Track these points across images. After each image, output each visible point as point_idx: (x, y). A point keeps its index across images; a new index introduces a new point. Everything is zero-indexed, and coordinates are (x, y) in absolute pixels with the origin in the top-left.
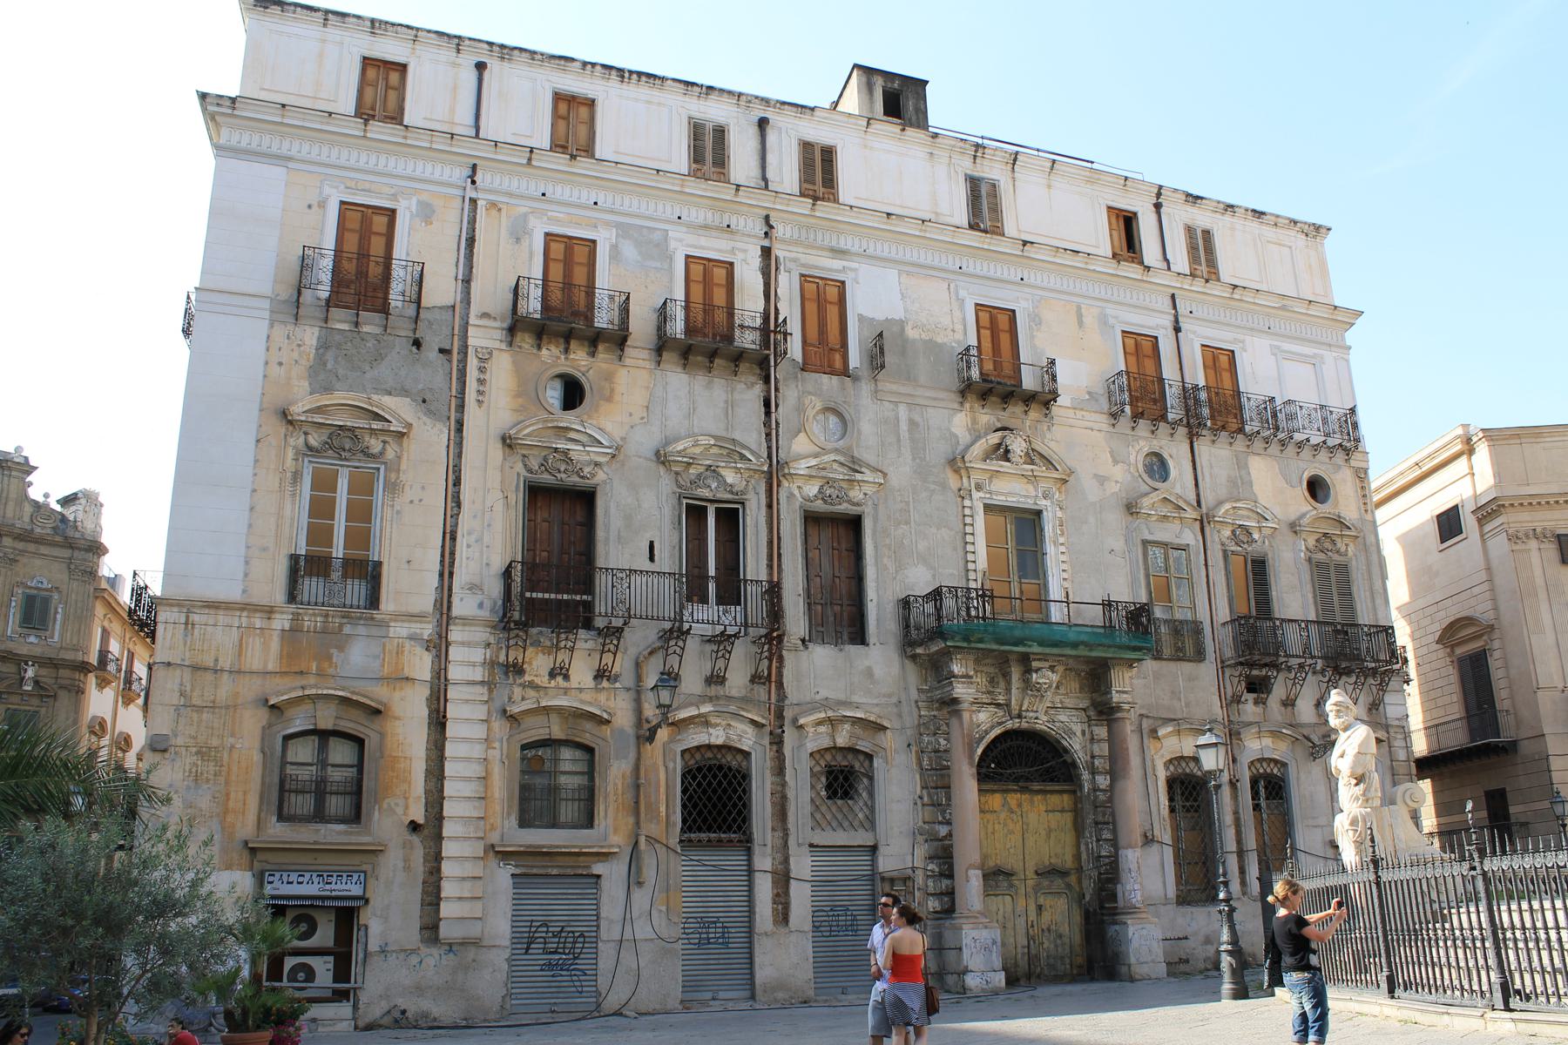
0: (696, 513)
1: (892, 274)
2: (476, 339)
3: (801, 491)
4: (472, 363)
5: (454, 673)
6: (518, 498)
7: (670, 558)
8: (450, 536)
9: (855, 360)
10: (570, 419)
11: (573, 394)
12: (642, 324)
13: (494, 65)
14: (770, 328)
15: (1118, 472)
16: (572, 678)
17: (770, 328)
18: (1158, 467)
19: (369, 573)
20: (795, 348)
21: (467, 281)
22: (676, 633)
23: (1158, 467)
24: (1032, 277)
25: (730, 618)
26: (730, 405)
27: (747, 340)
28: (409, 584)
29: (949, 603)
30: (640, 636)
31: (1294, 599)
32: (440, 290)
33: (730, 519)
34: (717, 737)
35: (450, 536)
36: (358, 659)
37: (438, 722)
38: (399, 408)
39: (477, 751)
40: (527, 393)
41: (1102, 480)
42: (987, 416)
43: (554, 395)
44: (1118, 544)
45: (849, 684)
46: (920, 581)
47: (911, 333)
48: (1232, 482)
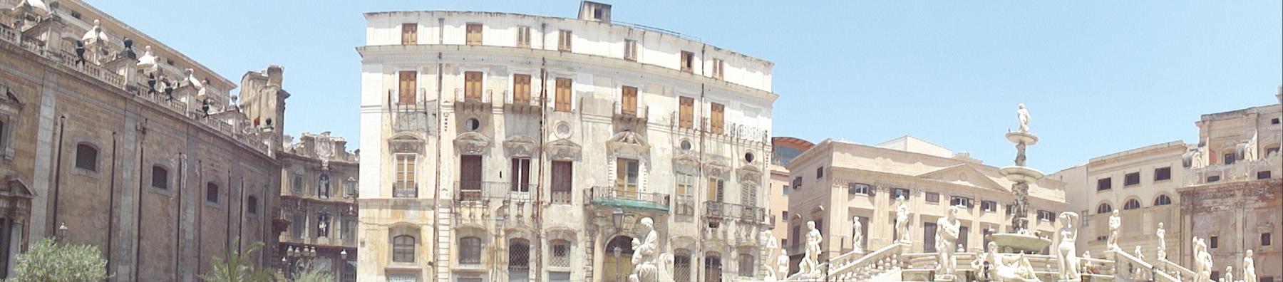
0: (515, 161)
2: (443, 110)
4: (443, 118)
5: (441, 216)
6: (458, 159)
7: (507, 177)
8: (438, 173)
9: (573, 107)
10: (473, 133)
11: (476, 125)
12: (497, 102)
13: (446, 18)
14: (543, 97)
16: (472, 215)
17: (543, 97)
20: (551, 104)
21: (440, 90)
22: (506, 203)
25: (526, 196)
26: (528, 124)
27: (535, 103)
28: (426, 193)
29: (596, 193)
30: (496, 204)
32: (432, 95)
33: (526, 163)
34: (519, 235)
35: (438, 173)
36: (412, 216)
37: (436, 229)
39: (447, 240)
40: (460, 128)
43: (470, 125)
45: (566, 216)
46: (591, 183)
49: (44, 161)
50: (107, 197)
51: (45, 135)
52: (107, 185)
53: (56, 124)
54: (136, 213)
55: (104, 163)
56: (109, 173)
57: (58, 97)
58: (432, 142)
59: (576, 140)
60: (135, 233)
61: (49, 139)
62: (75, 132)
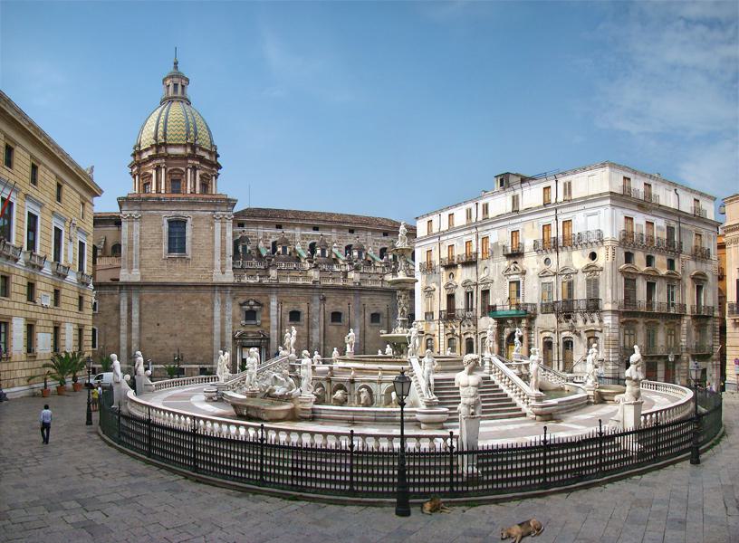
0: (467, 294)
1: (496, 231)
3: (481, 287)
15: (538, 266)
18: (547, 261)
19: (432, 313)
23: (547, 261)
24: (524, 219)
31: (580, 293)
33: (472, 293)
38: (433, 285)
41: (534, 269)
42: (512, 261)
44: (536, 285)
47: (500, 244)
48: (567, 260)
49: (274, 321)
50: (306, 331)
51: (273, 313)
52: (305, 326)
53: (278, 307)
54: (322, 336)
55: (304, 317)
56: (306, 321)
57: (278, 297)
58: (437, 289)
59: (491, 277)
60: (322, 343)
61: (276, 313)
62: (287, 308)
